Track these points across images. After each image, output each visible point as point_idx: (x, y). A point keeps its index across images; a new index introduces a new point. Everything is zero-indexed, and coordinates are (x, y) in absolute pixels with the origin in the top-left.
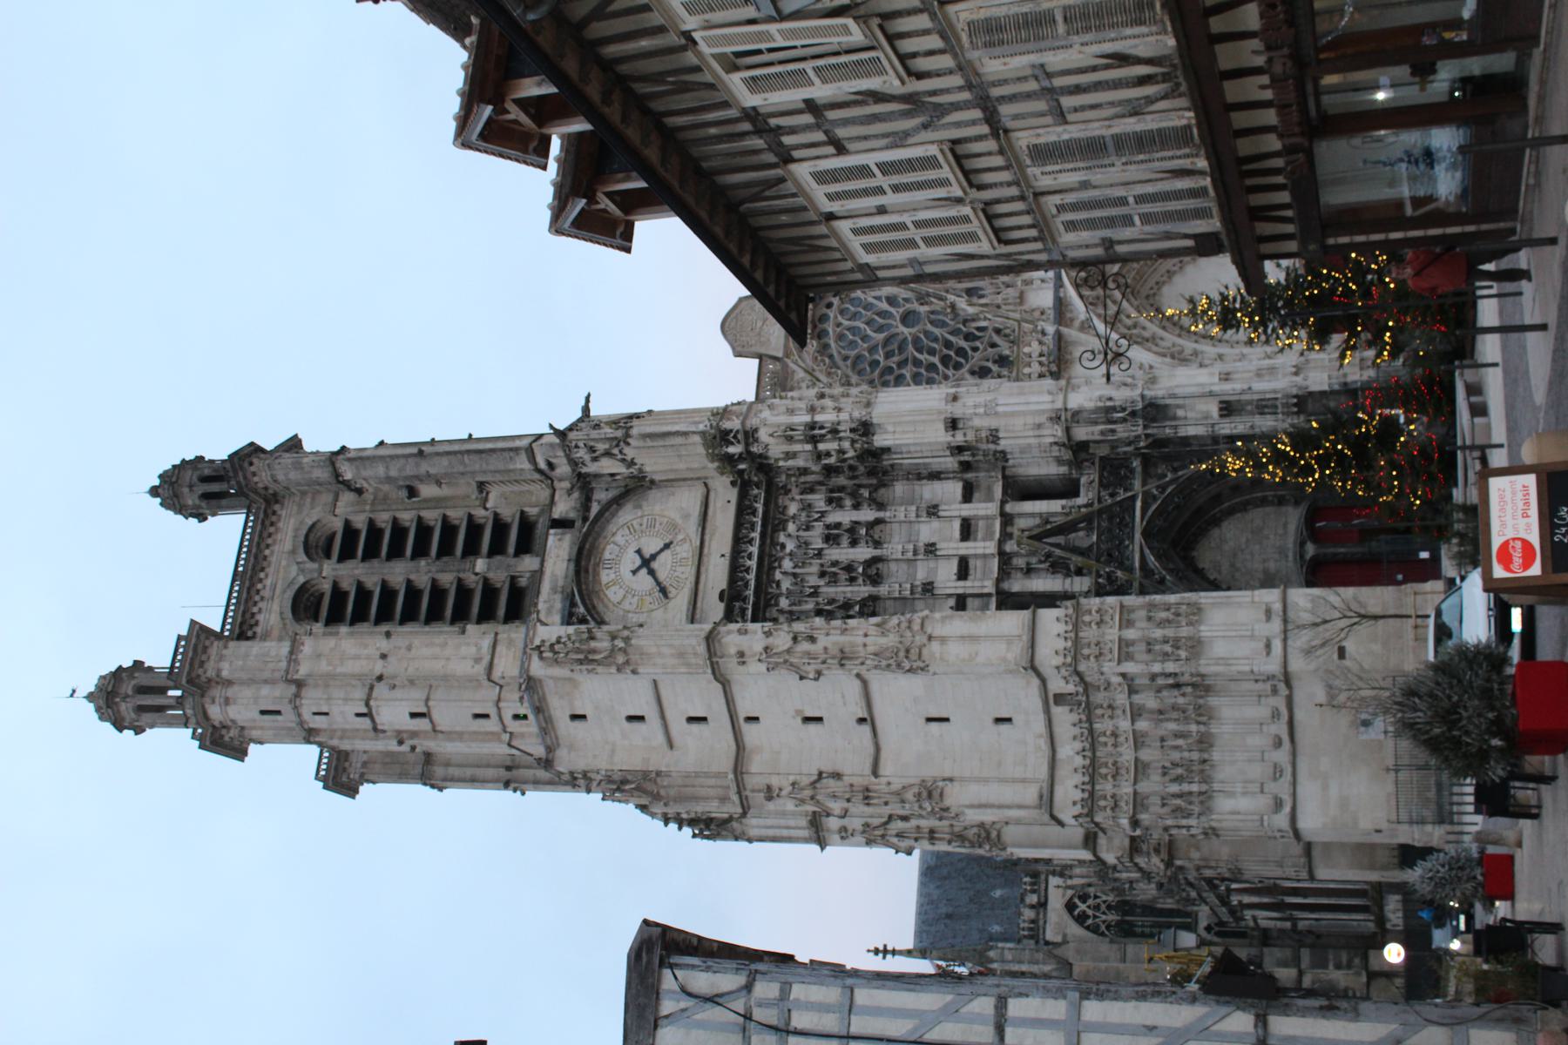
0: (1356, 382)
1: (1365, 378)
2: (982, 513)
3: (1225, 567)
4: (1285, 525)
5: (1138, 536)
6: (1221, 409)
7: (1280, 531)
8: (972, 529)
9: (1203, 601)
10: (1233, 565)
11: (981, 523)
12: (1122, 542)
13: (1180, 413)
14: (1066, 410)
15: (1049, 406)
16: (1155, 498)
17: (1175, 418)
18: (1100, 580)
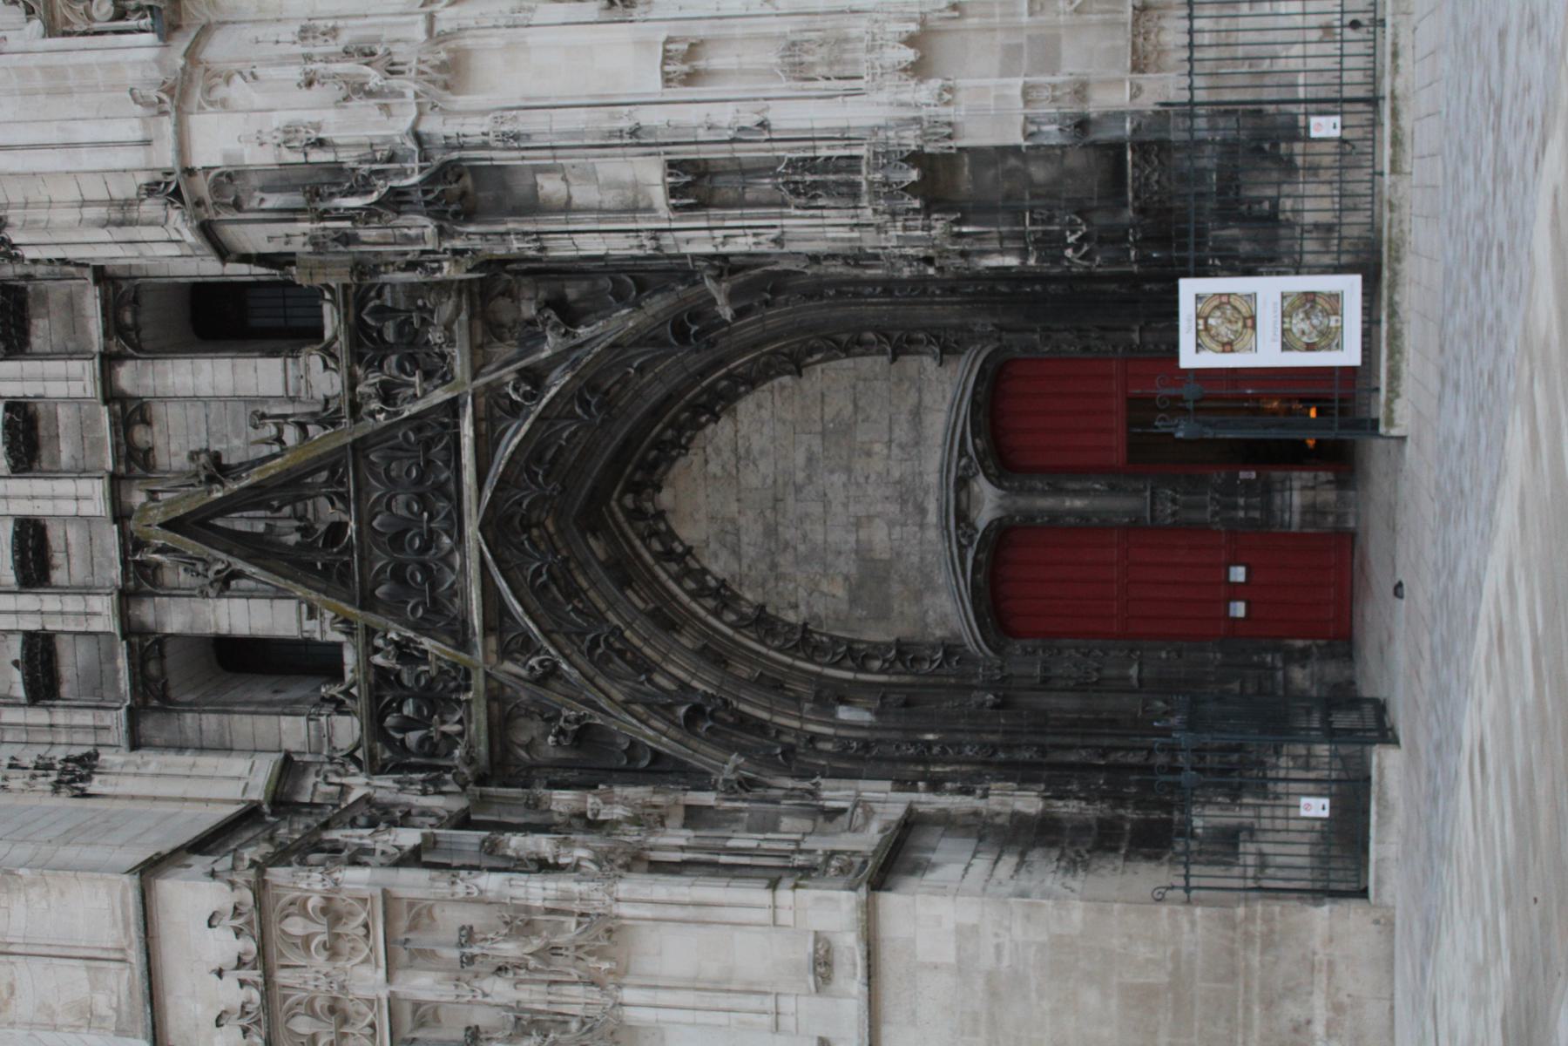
0: (1119, 116)
1: (1148, 102)
2: (56, 389)
3: (752, 533)
4: (917, 414)
5: (471, 529)
6: (673, 191)
7: (902, 433)
8: (42, 432)
9: (625, 910)
10: (771, 531)
11: (63, 413)
12: (430, 540)
13: (550, 187)
14: (189, 172)
15: (132, 158)
16: (515, 410)
17: (533, 206)
18: (378, 659)
